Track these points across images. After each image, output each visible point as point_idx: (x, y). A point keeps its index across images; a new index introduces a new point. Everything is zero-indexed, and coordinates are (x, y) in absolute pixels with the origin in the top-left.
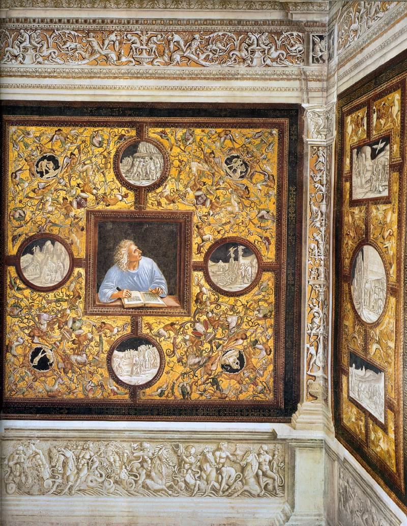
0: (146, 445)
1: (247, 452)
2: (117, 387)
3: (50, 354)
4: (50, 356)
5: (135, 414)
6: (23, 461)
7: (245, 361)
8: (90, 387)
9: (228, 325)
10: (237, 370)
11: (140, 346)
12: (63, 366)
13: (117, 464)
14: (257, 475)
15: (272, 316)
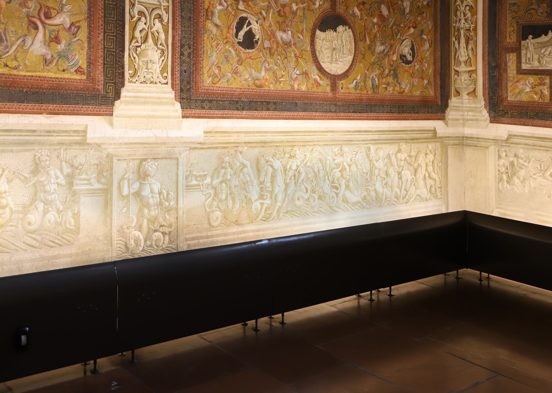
0: (346, 149)
1: (418, 152)
2: (320, 77)
3: (256, 27)
4: (255, 29)
5: (335, 112)
6: (229, 177)
7: (416, 52)
8: (296, 76)
9: (404, 11)
10: (410, 62)
11: (338, 26)
12: (269, 46)
13: (321, 175)
14: (425, 177)
15: (433, 6)
